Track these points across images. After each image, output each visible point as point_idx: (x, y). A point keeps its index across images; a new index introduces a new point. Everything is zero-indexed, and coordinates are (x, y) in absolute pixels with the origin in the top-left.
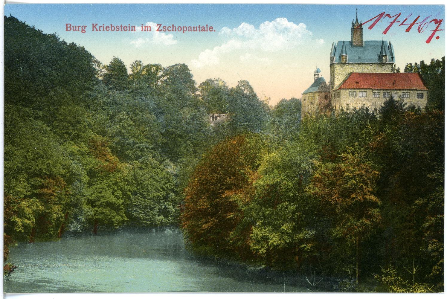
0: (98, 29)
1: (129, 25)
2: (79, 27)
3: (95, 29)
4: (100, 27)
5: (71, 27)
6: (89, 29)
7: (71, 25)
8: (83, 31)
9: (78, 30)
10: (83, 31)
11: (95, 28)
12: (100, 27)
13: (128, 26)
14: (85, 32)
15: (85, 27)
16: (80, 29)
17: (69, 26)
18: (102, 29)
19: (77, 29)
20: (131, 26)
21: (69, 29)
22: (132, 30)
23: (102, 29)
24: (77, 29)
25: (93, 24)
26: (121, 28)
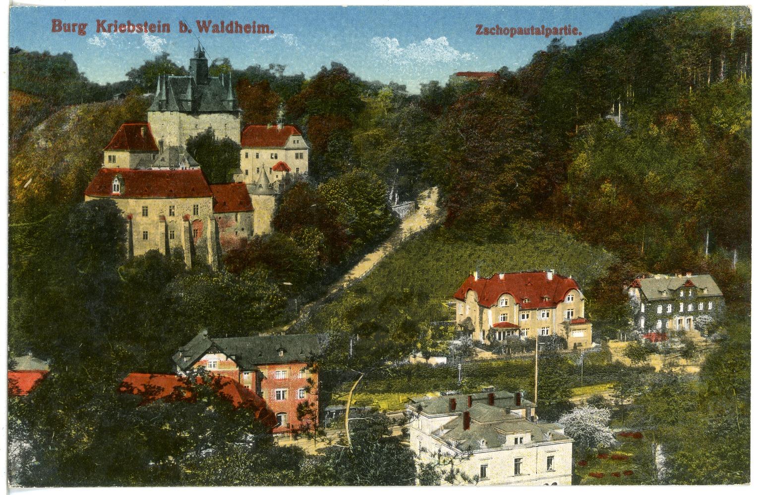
0: (107, 28)
1: (159, 22)
2: (74, 25)
3: (101, 29)
4: (110, 26)
5: (62, 25)
6: (92, 27)
7: (60, 22)
8: (82, 32)
9: (74, 30)
10: (82, 32)
11: (101, 29)
12: (110, 26)
13: (156, 24)
14: (84, 33)
15: (85, 25)
16: (77, 28)
17: (57, 23)
18: (113, 28)
19: (71, 28)
20: (161, 24)
21: (57, 28)
22: (164, 31)
23: (113, 28)
24: (71, 28)
25: (98, 21)
26: (146, 29)
